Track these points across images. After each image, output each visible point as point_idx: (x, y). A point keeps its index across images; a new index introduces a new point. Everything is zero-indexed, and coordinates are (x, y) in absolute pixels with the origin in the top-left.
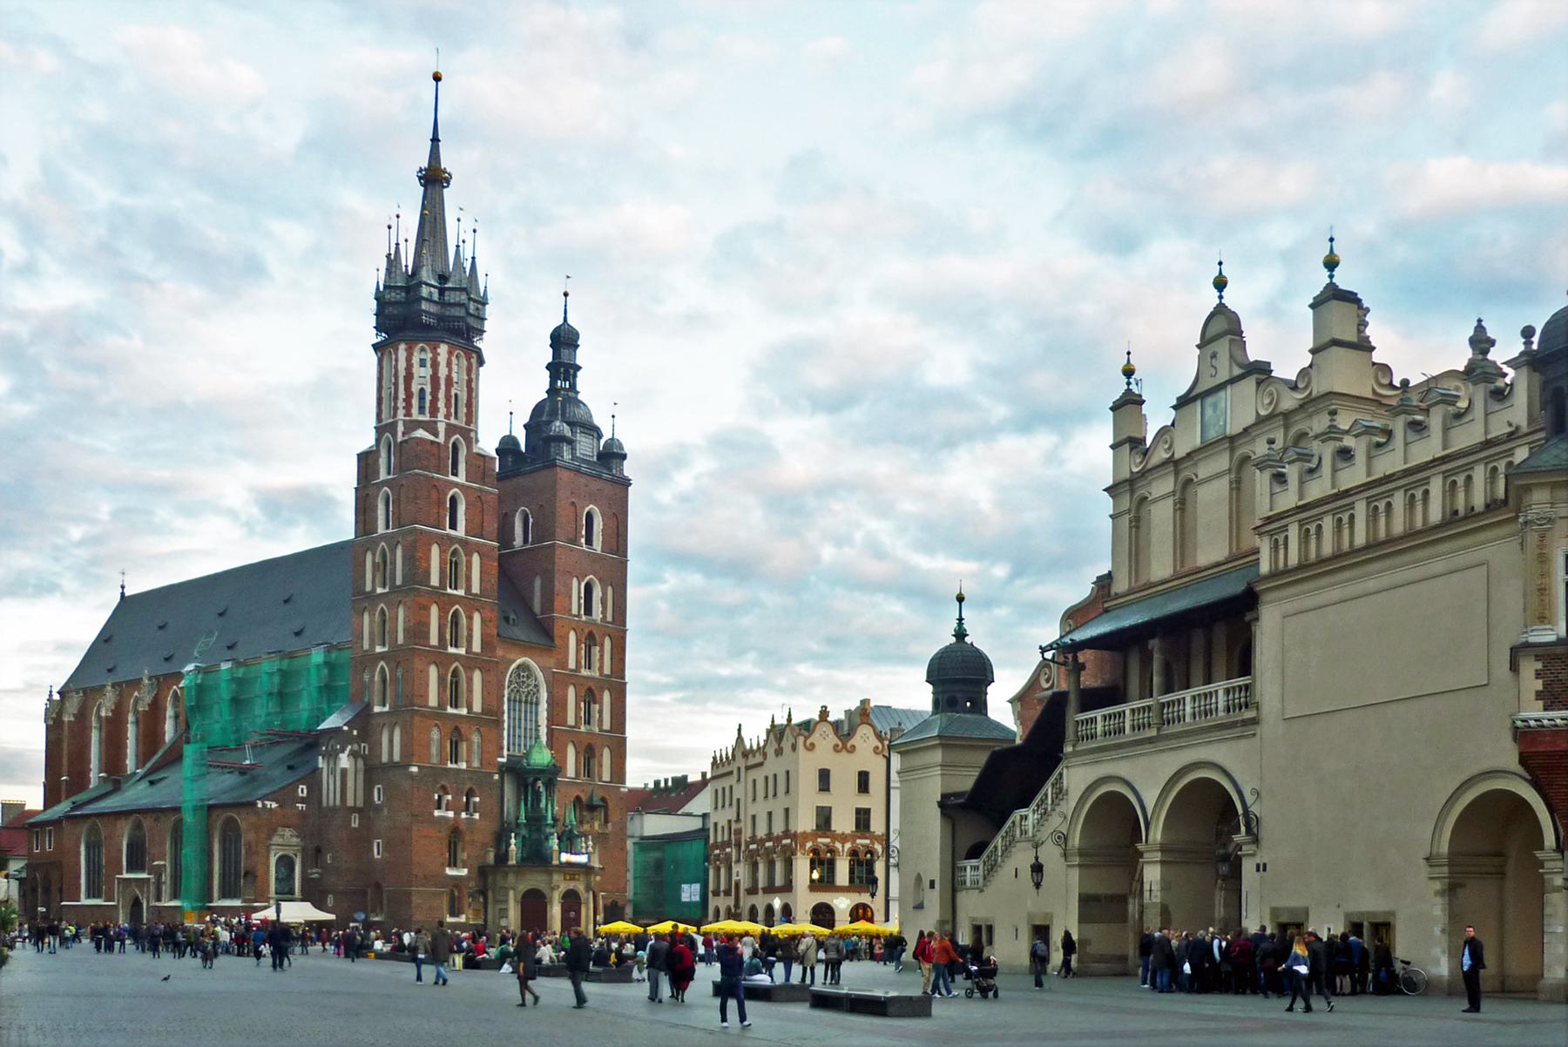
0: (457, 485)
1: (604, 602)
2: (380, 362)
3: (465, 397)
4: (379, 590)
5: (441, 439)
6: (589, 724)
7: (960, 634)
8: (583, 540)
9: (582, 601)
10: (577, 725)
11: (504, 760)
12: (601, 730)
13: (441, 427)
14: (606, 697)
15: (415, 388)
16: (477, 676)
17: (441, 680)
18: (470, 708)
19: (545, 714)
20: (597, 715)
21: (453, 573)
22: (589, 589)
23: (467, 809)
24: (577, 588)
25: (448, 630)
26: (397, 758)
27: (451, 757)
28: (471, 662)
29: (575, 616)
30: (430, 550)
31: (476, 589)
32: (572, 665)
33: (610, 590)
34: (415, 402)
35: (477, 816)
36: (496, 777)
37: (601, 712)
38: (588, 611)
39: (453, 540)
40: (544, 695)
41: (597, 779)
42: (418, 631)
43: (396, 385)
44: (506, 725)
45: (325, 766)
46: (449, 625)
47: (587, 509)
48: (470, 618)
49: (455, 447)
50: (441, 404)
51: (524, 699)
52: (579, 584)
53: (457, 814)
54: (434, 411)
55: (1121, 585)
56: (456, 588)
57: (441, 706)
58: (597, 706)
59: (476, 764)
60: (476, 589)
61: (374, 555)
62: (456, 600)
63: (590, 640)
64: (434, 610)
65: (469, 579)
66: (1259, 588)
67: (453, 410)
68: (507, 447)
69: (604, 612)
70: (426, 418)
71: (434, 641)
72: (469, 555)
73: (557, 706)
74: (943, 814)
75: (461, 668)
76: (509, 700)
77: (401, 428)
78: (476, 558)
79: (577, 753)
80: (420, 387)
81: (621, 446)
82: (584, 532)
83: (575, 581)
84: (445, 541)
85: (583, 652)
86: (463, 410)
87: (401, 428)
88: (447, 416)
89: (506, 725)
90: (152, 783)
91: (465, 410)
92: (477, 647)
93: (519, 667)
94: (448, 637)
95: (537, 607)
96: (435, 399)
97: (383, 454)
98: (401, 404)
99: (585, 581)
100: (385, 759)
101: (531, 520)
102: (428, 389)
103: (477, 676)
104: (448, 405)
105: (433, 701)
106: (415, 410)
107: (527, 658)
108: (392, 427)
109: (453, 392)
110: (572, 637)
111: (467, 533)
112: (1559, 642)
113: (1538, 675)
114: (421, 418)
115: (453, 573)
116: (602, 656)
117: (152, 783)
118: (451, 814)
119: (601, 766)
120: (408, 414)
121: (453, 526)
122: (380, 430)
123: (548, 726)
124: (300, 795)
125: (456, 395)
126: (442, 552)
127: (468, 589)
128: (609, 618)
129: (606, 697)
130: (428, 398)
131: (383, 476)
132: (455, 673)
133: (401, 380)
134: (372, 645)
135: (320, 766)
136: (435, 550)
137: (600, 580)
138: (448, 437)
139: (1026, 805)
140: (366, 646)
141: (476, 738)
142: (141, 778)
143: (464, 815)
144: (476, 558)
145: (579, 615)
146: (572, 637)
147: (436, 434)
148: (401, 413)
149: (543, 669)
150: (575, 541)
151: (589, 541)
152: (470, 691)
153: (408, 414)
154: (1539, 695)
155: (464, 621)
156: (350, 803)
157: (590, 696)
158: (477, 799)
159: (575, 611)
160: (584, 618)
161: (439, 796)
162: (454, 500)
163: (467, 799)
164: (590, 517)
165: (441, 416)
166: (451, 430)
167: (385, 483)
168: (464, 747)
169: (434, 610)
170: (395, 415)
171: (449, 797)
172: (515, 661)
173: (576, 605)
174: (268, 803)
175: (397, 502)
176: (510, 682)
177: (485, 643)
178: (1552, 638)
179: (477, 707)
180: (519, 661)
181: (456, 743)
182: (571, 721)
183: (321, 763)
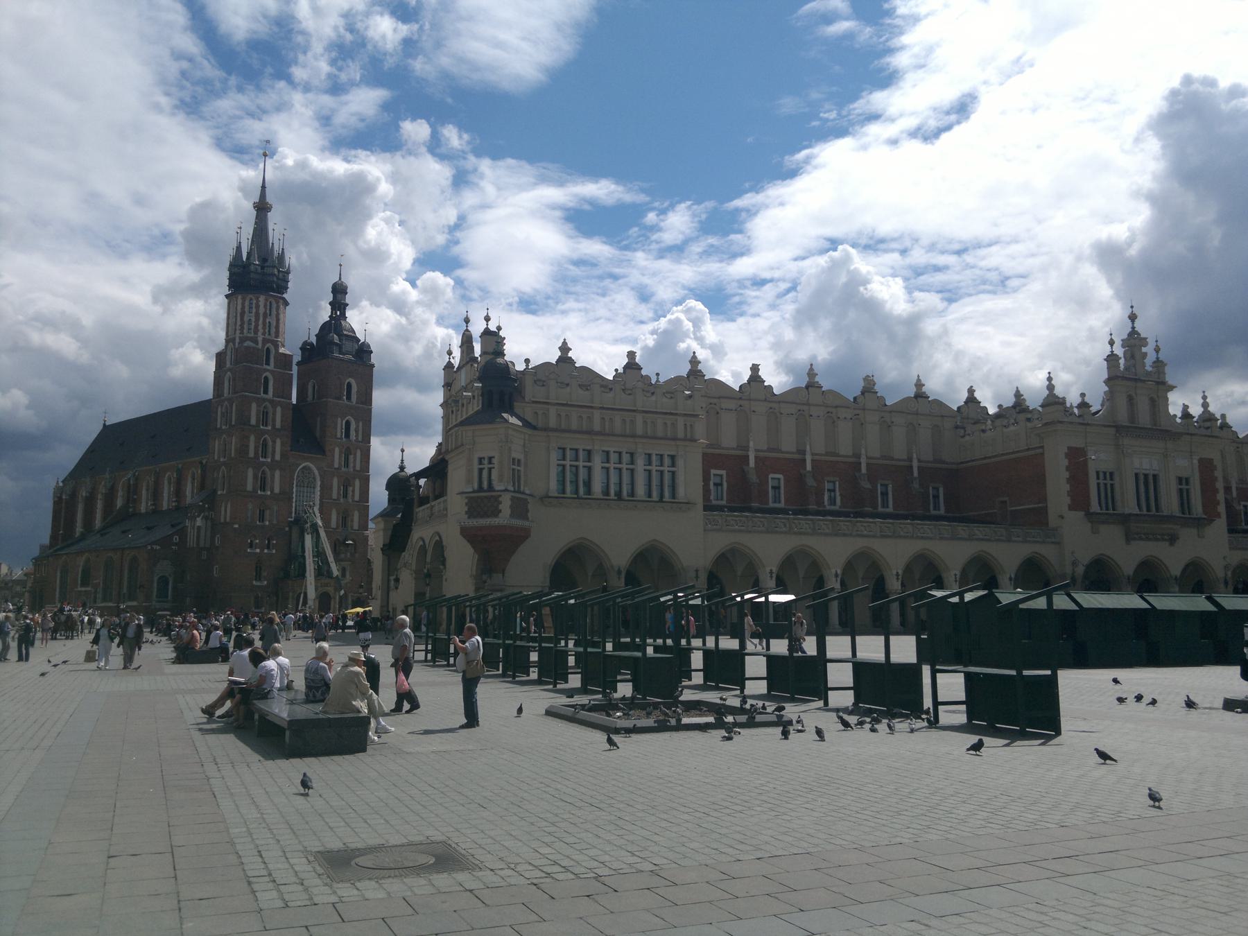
0: (268, 370)
1: (357, 431)
2: (229, 304)
3: (275, 324)
4: (224, 427)
5: (260, 345)
6: (346, 497)
7: (402, 468)
8: (345, 398)
9: (344, 431)
10: (338, 499)
11: (292, 520)
12: (353, 501)
13: (260, 339)
14: (357, 483)
15: (246, 319)
16: (277, 474)
17: (255, 477)
18: (272, 491)
19: (319, 493)
20: (351, 493)
21: (264, 417)
22: (348, 424)
23: (268, 548)
24: (340, 424)
25: (261, 449)
26: (228, 520)
27: (260, 518)
28: (274, 465)
29: (339, 439)
30: (251, 406)
31: (278, 425)
32: (336, 465)
33: (361, 424)
34: (246, 326)
35: (274, 551)
36: (287, 529)
37: (353, 491)
38: (347, 435)
39: (264, 400)
40: (319, 483)
41: (349, 529)
42: (243, 450)
43: (236, 316)
44: (294, 500)
45: (189, 525)
46: (261, 446)
47: (347, 381)
48: (274, 442)
49: (268, 349)
50: (260, 327)
51: (306, 485)
52: (342, 421)
53: (262, 550)
54: (256, 331)
55: (443, 450)
56: (266, 426)
57: (255, 490)
58: (351, 488)
59: (275, 522)
60: (278, 425)
61: (222, 408)
62: (266, 432)
63: (347, 453)
64: (252, 438)
65: (274, 420)
66: (447, 457)
67: (267, 331)
68: (306, 348)
69: (357, 436)
70: (252, 335)
71: (251, 454)
72: (274, 407)
73: (326, 489)
74: (383, 554)
75: (267, 470)
76: (297, 486)
77: (237, 340)
78: (279, 409)
79: (338, 514)
80: (249, 318)
81: (369, 346)
82: (345, 394)
83: (339, 419)
84: (260, 401)
85: (343, 459)
86: (273, 330)
87: (237, 340)
88: (264, 334)
89: (294, 500)
90: (102, 535)
91: (274, 330)
92: (278, 457)
93: (304, 468)
94: (260, 452)
95: (318, 434)
96: (257, 326)
97: (229, 353)
98: (238, 327)
99: (346, 419)
100: (222, 520)
101: (316, 387)
102: (253, 319)
103: (277, 474)
104: (264, 328)
105: (249, 487)
106: (245, 331)
107: (308, 463)
108: (233, 340)
109: (267, 321)
110: (337, 450)
111: (273, 396)
112: (473, 492)
113: (466, 504)
114: (249, 335)
115: (264, 417)
116: (355, 460)
117: (102, 535)
118: (258, 551)
119: (352, 521)
120: (242, 332)
121: (266, 392)
122: (227, 341)
123: (320, 500)
124: (175, 541)
125: (269, 322)
126: (258, 406)
127: (274, 426)
128: (360, 439)
129: (357, 483)
130: (253, 324)
131: (228, 365)
132: (263, 472)
133: (239, 315)
134: (219, 457)
135: (187, 524)
136: (254, 406)
137: (355, 419)
138: (264, 344)
139: (404, 551)
140: (216, 458)
141: (275, 508)
142: (98, 532)
143: (266, 551)
144: (279, 409)
145: (341, 438)
146: (337, 450)
147: (256, 342)
148: (238, 332)
149: (318, 469)
150: (340, 398)
151: (349, 398)
152: (273, 481)
153: (242, 332)
154: (466, 513)
155: (270, 443)
156: (202, 544)
157: (346, 485)
158: (275, 542)
159: (339, 436)
160: (344, 439)
161: (251, 541)
162: (266, 378)
163: (269, 542)
164: (349, 385)
165: (260, 334)
166: (265, 341)
167: (229, 370)
168: (267, 513)
169: (252, 438)
170: (235, 333)
171: (257, 541)
172: (300, 464)
173: (340, 432)
174: (155, 547)
175: (234, 380)
176: (298, 476)
177: (282, 455)
178: (471, 490)
179: (277, 490)
180: (303, 465)
181: (263, 511)
182: (335, 496)
183: (188, 523)
